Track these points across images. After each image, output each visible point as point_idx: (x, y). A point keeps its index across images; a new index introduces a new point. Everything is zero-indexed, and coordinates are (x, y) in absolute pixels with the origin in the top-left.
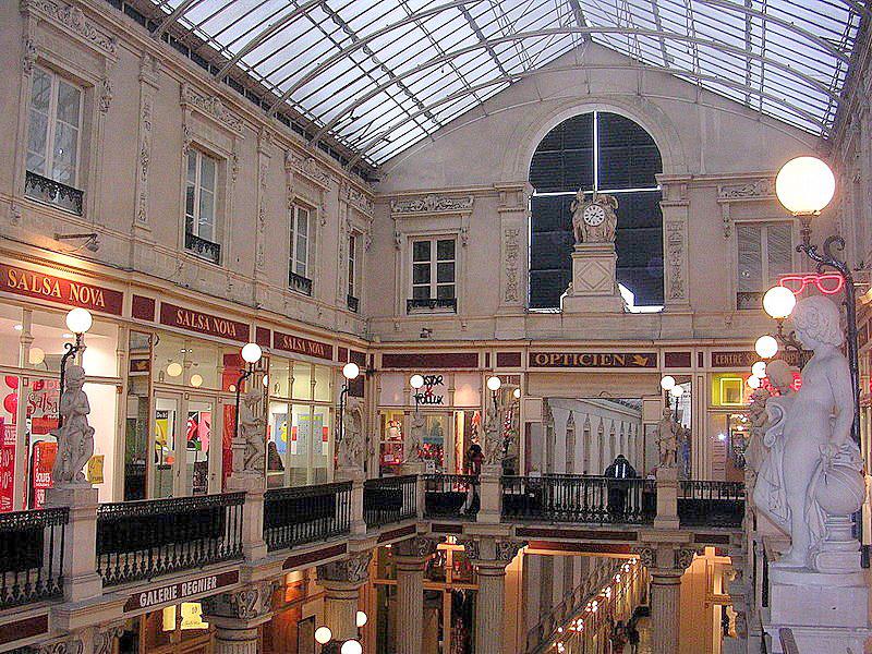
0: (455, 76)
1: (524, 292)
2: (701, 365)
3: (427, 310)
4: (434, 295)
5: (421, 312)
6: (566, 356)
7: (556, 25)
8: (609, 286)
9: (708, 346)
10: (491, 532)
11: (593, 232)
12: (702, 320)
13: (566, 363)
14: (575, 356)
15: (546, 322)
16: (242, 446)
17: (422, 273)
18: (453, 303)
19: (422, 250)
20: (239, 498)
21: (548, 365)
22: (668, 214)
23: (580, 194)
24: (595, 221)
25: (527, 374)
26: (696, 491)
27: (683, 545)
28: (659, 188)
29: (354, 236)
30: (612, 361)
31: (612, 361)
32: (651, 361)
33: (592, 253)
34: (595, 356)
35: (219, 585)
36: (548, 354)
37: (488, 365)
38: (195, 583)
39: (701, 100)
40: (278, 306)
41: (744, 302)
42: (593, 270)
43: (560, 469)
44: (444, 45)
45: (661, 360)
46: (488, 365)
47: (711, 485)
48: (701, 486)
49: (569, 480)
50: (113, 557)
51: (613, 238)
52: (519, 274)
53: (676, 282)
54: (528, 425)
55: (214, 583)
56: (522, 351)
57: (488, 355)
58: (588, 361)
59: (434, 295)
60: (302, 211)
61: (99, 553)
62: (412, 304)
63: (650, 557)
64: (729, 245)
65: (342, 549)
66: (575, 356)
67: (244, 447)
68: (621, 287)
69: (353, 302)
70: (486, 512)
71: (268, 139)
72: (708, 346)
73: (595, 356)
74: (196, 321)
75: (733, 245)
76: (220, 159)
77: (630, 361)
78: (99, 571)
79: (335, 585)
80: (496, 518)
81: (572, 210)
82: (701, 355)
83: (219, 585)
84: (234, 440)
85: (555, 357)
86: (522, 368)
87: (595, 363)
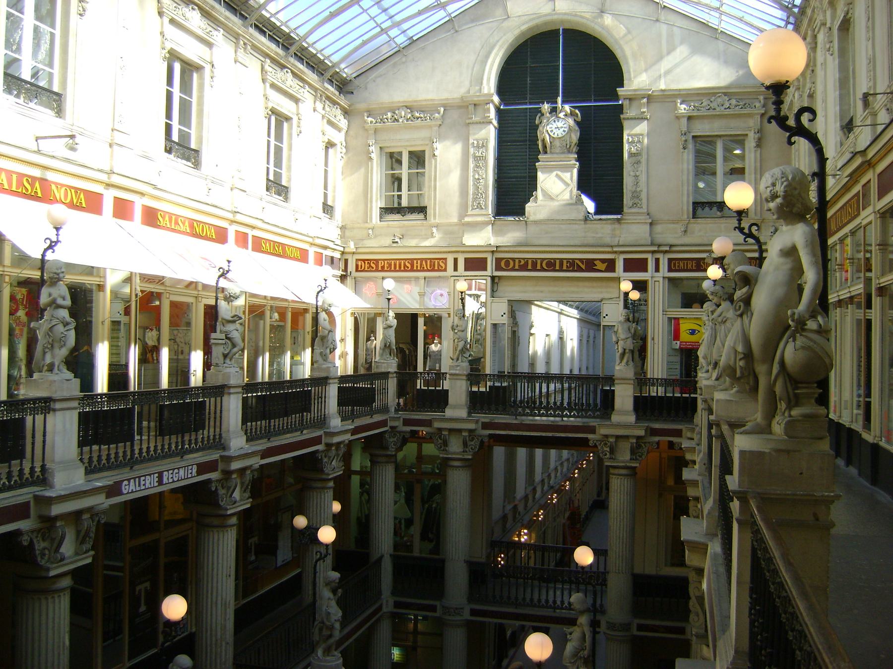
2: (657, 270)
3: (398, 217)
4: (404, 203)
9: (666, 252)
11: (557, 143)
13: (530, 267)
14: (539, 262)
16: (220, 341)
18: (422, 210)
19: (394, 159)
20: (219, 391)
21: (513, 269)
23: (546, 107)
24: (559, 133)
25: (493, 278)
26: (651, 388)
27: (638, 438)
28: (620, 103)
30: (573, 265)
31: (573, 265)
32: (610, 265)
34: (558, 262)
35: (199, 473)
36: (514, 259)
37: (456, 269)
38: (176, 471)
39: (662, 18)
41: (699, 211)
45: (620, 265)
46: (456, 269)
47: (666, 383)
48: (654, 382)
51: (575, 149)
55: (195, 471)
57: (456, 260)
58: (551, 265)
60: (279, 119)
62: (387, 211)
63: (608, 449)
64: (685, 155)
65: (317, 441)
66: (539, 262)
67: (223, 342)
68: (584, 198)
70: (455, 407)
71: (245, 49)
72: (666, 252)
74: (177, 223)
75: (688, 157)
77: (590, 265)
78: (81, 460)
80: (463, 413)
81: (537, 122)
82: (657, 261)
83: (199, 473)
84: (213, 335)
85: (520, 262)
87: (557, 268)
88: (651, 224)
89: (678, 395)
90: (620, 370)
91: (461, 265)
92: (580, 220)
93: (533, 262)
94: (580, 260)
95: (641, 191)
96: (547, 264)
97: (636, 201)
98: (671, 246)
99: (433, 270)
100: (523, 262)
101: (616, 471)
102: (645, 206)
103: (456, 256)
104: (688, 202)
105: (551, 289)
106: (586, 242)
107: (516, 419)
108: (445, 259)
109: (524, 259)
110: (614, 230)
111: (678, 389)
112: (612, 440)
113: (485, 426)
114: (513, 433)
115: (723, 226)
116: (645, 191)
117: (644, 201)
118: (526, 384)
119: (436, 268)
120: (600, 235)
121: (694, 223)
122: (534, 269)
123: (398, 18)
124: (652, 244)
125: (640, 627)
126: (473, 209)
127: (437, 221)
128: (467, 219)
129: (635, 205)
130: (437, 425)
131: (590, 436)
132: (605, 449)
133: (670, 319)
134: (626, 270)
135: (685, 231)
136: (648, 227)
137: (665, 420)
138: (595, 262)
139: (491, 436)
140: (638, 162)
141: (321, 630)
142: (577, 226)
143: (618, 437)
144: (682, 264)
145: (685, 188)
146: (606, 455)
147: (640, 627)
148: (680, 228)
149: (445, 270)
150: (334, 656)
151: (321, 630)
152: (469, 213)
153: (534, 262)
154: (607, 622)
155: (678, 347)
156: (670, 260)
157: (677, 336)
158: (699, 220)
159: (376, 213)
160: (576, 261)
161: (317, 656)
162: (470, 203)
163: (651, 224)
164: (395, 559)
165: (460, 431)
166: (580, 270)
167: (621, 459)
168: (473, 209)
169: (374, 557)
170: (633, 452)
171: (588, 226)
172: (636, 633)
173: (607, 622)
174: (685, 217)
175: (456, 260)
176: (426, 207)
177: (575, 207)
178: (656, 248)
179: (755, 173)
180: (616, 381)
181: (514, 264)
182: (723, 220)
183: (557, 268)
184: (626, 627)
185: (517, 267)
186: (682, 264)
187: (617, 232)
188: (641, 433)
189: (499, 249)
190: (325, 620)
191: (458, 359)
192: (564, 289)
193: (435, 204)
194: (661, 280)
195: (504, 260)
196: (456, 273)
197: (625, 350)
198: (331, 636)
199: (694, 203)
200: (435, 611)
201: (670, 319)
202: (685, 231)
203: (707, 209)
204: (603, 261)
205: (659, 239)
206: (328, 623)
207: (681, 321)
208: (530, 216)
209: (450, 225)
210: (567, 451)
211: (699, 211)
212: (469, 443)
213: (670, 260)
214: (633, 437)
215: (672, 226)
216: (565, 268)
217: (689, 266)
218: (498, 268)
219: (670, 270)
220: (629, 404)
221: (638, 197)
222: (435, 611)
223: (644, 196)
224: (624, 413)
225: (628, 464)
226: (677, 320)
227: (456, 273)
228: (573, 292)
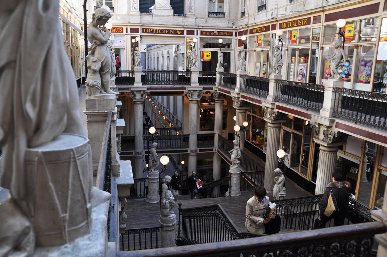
2: (197, 34)
6: (154, 30)
12: (197, 20)
13: (154, 32)
15: (146, 19)
21: (148, 33)
25: (141, 35)
27: (200, 91)
30: (169, 32)
31: (169, 32)
32: (182, 32)
34: (164, 30)
36: (148, 29)
37: (127, 32)
45: (185, 32)
46: (127, 32)
53: (190, 7)
56: (140, 28)
57: (127, 29)
58: (162, 32)
63: (190, 95)
70: (137, 83)
73: (164, 30)
77: (175, 32)
82: (197, 31)
85: (151, 30)
87: (164, 33)
88: (195, 18)
89: (201, 76)
90: (194, 69)
91: (129, 30)
92: (172, 16)
93: (155, 30)
94: (172, 30)
95: (192, 7)
96: (160, 31)
97: (191, 10)
98: (202, 26)
99: (118, 32)
100: (152, 30)
101: (192, 102)
102: (193, 12)
103: (127, 27)
104: (207, 11)
105: (161, 40)
106: (174, 24)
107: (159, 86)
108: (123, 28)
109: (152, 29)
110: (183, 20)
111: (201, 74)
112: (192, 92)
113: (149, 89)
114: (159, 91)
115: (218, 21)
116: (193, 7)
117: (193, 10)
118: (173, 74)
119: (119, 31)
120: (178, 21)
121: (209, 19)
122: (156, 33)
124: (196, 26)
125: (200, 150)
126: (132, 9)
127: (119, 13)
128: (131, 13)
129: (190, 11)
130: (132, 89)
131: (184, 91)
132: (189, 95)
133: (200, 51)
134: (187, 34)
135: (206, 22)
136: (194, 19)
137: (207, 85)
138: (177, 31)
139: (151, 92)
141: (153, 163)
142: (170, 18)
143: (194, 91)
144: (205, 33)
145: (206, 7)
146: (189, 97)
147: (200, 150)
148: (204, 20)
149: (123, 32)
150: (156, 171)
151: (153, 163)
152: (131, 11)
153: (156, 31)
154: (190, 150)
155: (202, 61)
156: (201, 31)
157: (203, 57)
158: (211, 18)
160: (171, 30)
161: (152, 172)
162: (131, 7)
163: (195, 18)
165: (140, 91)
166: (172, 34)
167: (194, 98)
168: (132, 9)
170: (198, 96)
171: (174, 18)
172: (199, 152)
173: (190, 150)
174: (206, 17)
175: (127, 29)
176: (114, 7)
177: (170, 11)
178: (198, 27)
179: (228, 4)
180: (192, 72)
181: (149, 31)
182: (217, 19)
183: (164, 33)
184: (196, 151)
185: (150, 32)
186: (205, 33)
187: (184, 21)
188: (201, 89)
189: (144, 25)
190: (156, 159)
191: (137, 66)
192: (165, 40)
193: (117, 6)
194: (198, 38)
195: (145, 29)
196: (127, 34)
197: (195, 62)
198: (156, 164)
199: (209, 12)
200: (133, 154)
201: (200, 51)
202: (206, 22)
203: (212, 14)
204: (180, 31)
205: (198, 24)
206: (157, 160)
207: (204, 52)
208: (154, 13)
209: (124, 15)
210: (166, 96)
211: (210, 15)
212: (143, 95)
213: (201, 31)
214: (199, 90)
215: (202, 19)
216: (167, 33)
217: (207, 34)
218: (143, 32)
219: (201, 35)
220: (197, 80)
221: (191, 9)
222: (133, 154)
223: (193, 8)
224: (195, 83)
225: (197, 100)
226: (203, 52)
227: (127, 34)
228: (168, 41)
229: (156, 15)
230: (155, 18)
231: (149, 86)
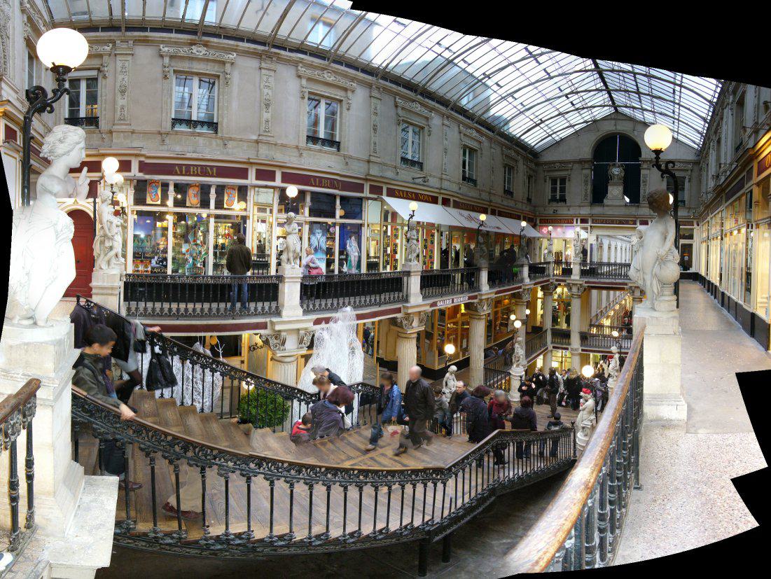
0: (565, 121)
1: (590, 198)
4: (558, 198)
5: (555, 204)
7: (594, 88)
8: (620, 196)
10: (576, 282)
11: (616, 177)
17: (554, 190)
18: (565, 201)
19: (554, 181)
22: (643, 172)
23: (611, 163)
24: (617, 173)
25: (591, 226)
29: (530, 177)
33: (615, 184)
40: (499, 201)
42: (615, 191)
43: (605, 260)
44: (571, 122)
49: (609, 264)
50: (431, 288)
52: (589, 191)
54: (591, 245)
59: (558, 198)
61: (421, 288)
62: (550, 201)
68: (625, 197)
69: (529, 200)
70: (575, 275)
76: (476, 151)
79: (518, 300)
80: (578, 278)
86: (589, 224)
113: (586, 282)
123: (555, 131)
130: (568, 281)
131: (625, 286)
139: (588, 286)
140: (646, 185)
159: (547, 201)
164: (552, 330)
166: (623, 224)
169: (544, 330)
229: (607, 206)
230: (605, 208)
231: (586, 280)
